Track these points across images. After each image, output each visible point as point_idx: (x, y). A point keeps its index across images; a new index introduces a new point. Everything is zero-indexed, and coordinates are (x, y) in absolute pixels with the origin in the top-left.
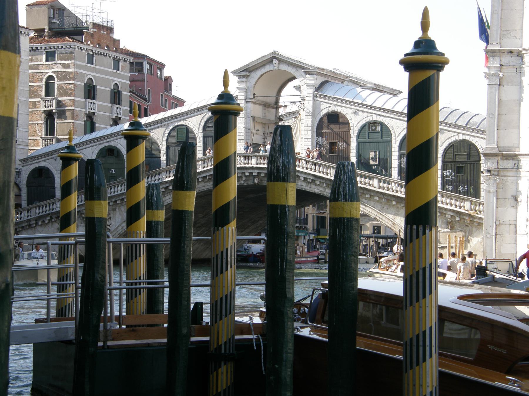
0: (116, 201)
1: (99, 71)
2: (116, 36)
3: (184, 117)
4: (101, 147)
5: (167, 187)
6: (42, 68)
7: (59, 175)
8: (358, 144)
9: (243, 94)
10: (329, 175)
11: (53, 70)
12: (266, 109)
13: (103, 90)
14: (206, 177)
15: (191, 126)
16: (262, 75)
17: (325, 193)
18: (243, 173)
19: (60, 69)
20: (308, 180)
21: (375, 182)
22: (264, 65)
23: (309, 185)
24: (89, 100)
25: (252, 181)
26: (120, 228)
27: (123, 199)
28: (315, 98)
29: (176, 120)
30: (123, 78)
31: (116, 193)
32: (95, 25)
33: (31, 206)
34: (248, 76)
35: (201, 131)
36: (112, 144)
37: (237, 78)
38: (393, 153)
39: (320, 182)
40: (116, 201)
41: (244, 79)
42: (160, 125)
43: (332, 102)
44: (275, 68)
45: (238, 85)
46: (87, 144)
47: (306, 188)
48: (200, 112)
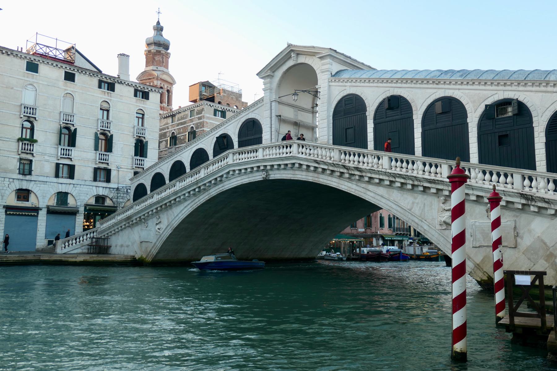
2: (244, 100)
3: (225, 126)
6: (188, 123)
8: (375, 124)
9: (268, 94)
10: (332, 159)
11: (194, 123)
12: (299, 112)
15: (230, 133)
21: (385, 161)
27: (166, 204)
28: (331, 84)
32: (224, 91)
34: (273, 76)
37: (262, 80)
41: (268, 80)
43: (346, 84)
45: (263, 87)
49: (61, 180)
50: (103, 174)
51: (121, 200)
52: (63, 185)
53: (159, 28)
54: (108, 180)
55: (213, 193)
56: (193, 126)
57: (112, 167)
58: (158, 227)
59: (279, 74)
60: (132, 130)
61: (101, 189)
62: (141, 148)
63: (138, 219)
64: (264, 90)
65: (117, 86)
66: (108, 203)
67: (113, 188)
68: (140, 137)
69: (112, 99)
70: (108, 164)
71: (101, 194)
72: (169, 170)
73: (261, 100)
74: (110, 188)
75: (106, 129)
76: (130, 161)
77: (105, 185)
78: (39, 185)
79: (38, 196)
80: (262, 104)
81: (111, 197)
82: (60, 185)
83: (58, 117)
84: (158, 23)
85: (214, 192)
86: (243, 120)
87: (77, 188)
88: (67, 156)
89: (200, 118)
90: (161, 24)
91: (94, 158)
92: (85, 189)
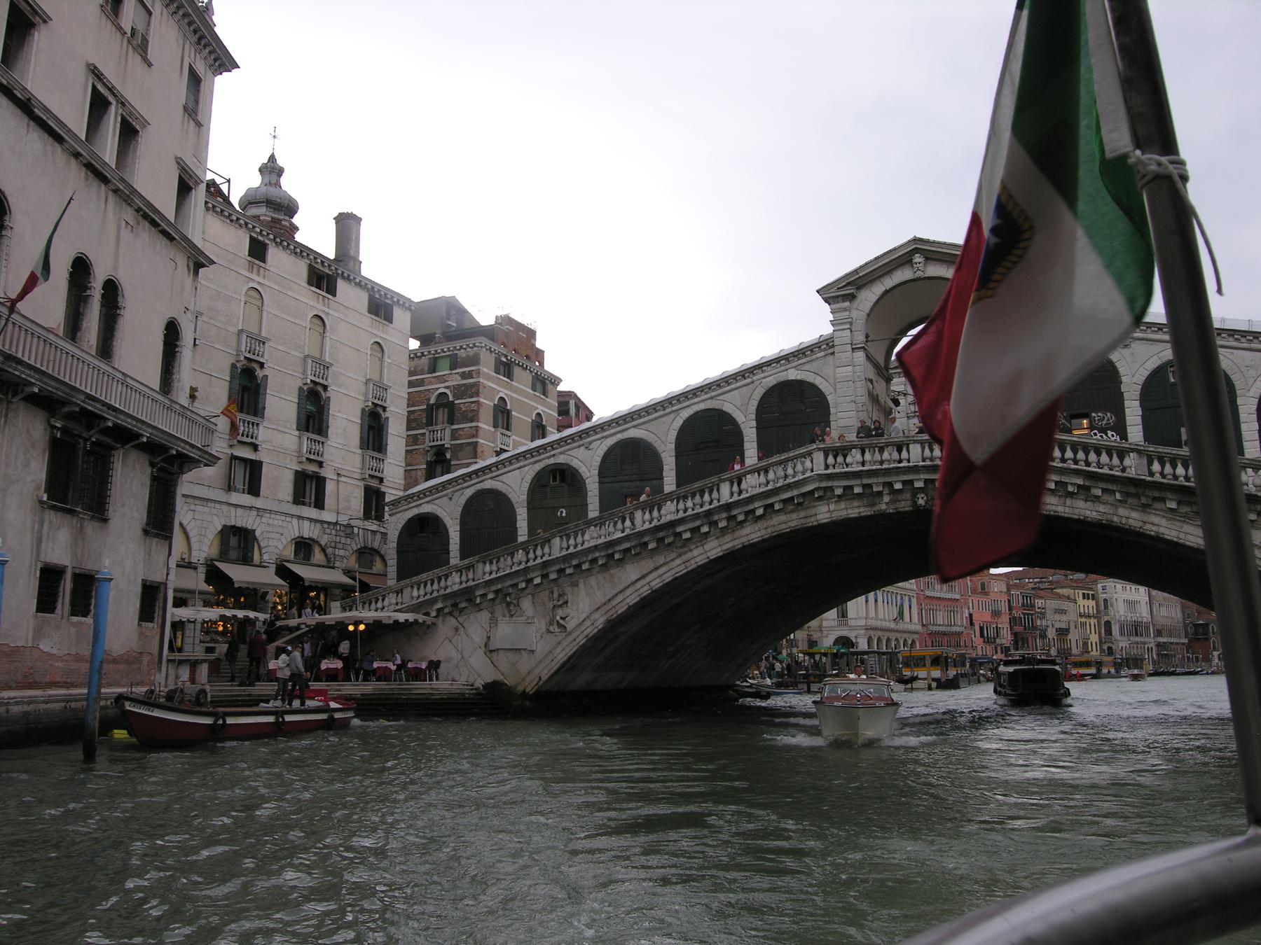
0: (578, 566)
1: (516, 390)
4: (538, 467)
5: (698, 528)
6: (431, 383)
7: (458, 528)
11: (447, 384)
13: (522, 418)
14: (792, 499)
15: (727, 408)
16: (886, 292)
17: (1115, 519)
18: (885, 484)
19: (456, 381)
20: (1070, 489)
22: (890, 272)
23: (1068, 502)
24: (500, 430)
25: (909, 503)
26: (588, 623)
27: (594, 561)
29: (696, 400)
30: (549, 412)
31: (579, 548)
33: (402, 583)
35: (754, 417)
36: (561, 459)
38: (1244, 427)
39: (1104, 490)
40: (578, 566)
41: (847, 304)
42: (662, 413)
44: (919, 274)
46: (511, 464)
47: (1060, 509)
48: (748, 380)
49: (236, 498)
50: (309, 487)
51: (342, 552)
52: (240, 511)
53: (272, 170)
54: (319, 504)
55: (753, 536)
56: (448, 391)
57: (327, 473)
58: (560, 613)
59: (869, 297)
60: (363, 389)
61: (306, 523)
62: (373, 430)
63: (491, 596)
64: (833, 323)
65: (341, 285)
66: (318, 556)
67: (329, 523)
68: (375, 405)
69: (331, 312)
70: (320, 464)
71: (306, 536)
72: (526, 485)
73: (825, 345)
74: (322, 522)
75: (322, 381)
76: (358, 459)
77: (312, 512)
78: (192, 507)
79: (191, 534)
80: (830, 351)
81: (323, 543)
82: (232, 509)
83: (234, 344)
84: (272, 158)
85: (752, 533)
86: (771, 381)
87: (264, 520)
88: (249, 440)
89: (464, 376)
90: (281, 162)
91: (295, 447)
92: (278, 521)
